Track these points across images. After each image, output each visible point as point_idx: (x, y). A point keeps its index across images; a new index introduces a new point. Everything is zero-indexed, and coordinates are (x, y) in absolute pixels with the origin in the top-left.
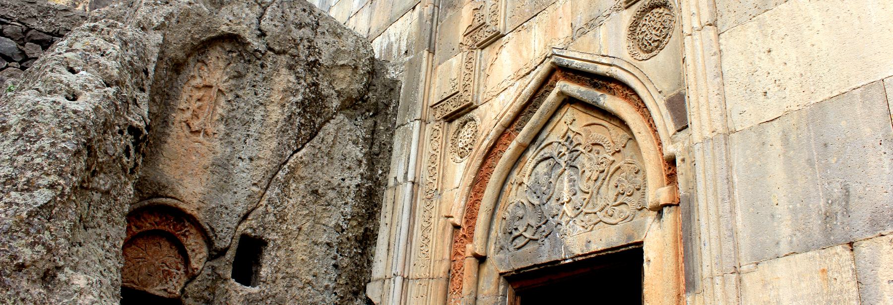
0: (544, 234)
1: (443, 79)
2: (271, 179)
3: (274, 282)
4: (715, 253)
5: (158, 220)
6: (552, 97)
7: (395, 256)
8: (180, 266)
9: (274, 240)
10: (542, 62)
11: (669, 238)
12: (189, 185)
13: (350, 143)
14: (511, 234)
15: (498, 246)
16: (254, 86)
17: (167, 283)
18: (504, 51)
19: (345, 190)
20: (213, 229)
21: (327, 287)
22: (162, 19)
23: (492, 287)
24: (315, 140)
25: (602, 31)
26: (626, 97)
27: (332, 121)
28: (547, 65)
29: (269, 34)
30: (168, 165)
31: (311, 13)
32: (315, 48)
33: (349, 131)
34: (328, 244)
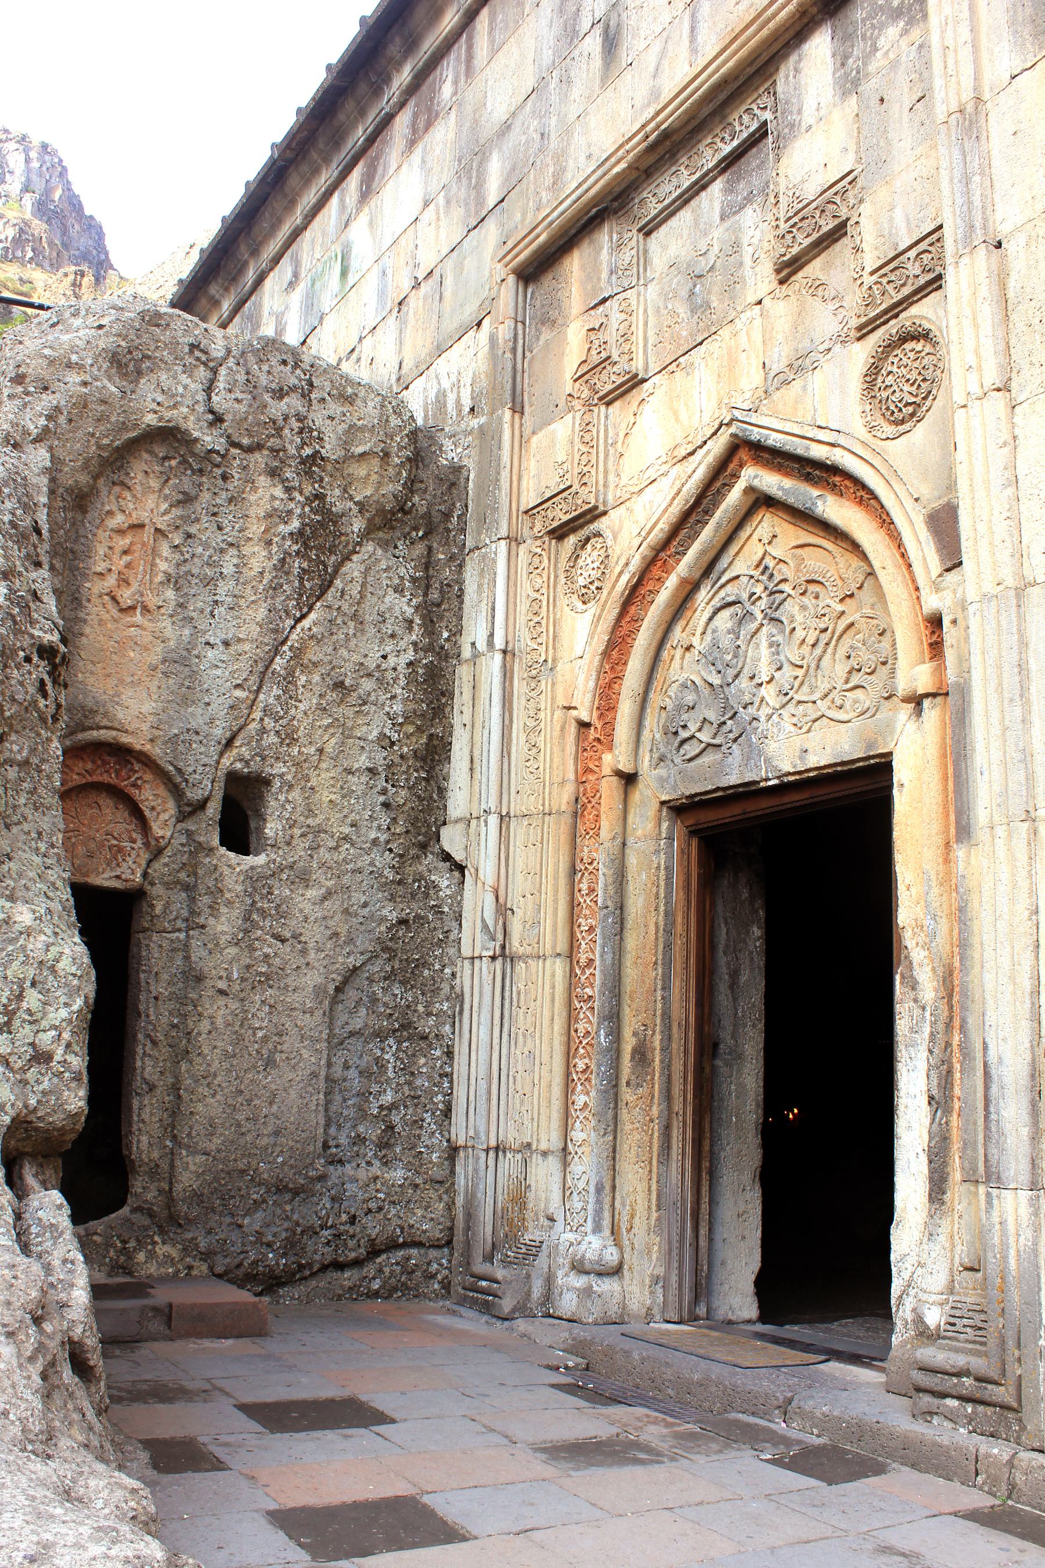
0: (731, 736)
1: (542, 461)
3: (288, 844)
5: (89, 766)
6: (734, 496)
7: (484, 780)
8: (134, 835)
9: (282, 776)
10: (715, 433)
12: (131, 703)
13: (390, 591)
15: (656, 756)
16: (214, 514)
17: (118, 865)
19: (390, 675)
20: (179, 771)
21: (375, 842)
22: (42, 421)
23: (650, 826)
25: (817, 380)
26: (860, 502)
27: (355, 558)
29: (228, 417)
30: (92, 673)
31: (296, 366)
32: (311, 430)
33: (385, 570)
34: (370, 770)
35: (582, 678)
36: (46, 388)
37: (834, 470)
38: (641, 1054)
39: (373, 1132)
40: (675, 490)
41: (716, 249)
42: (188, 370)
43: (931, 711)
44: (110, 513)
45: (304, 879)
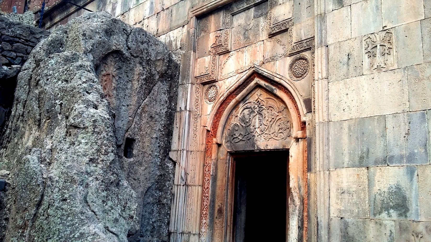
1: (201, 65)
3: (138, 156)
4: (321, 163)
6: (252, 84)
7: (183, 142)
9: (138, 139)
11: (301, 150)
14: (232, 135)
16: (126, 73)
18: (231, 59)
21: (156, 155)
22: (91, 47)
23: (224, 157)
24: (150, 94)
26: (285, 92)
27: (156, 85)
31: (146, 36)
34: (156, 138)
35: (208, 120)
36: (91, 38)
37: (280, 84)
41: (252, 25)
42: (123, 35)
45: (141, 164)
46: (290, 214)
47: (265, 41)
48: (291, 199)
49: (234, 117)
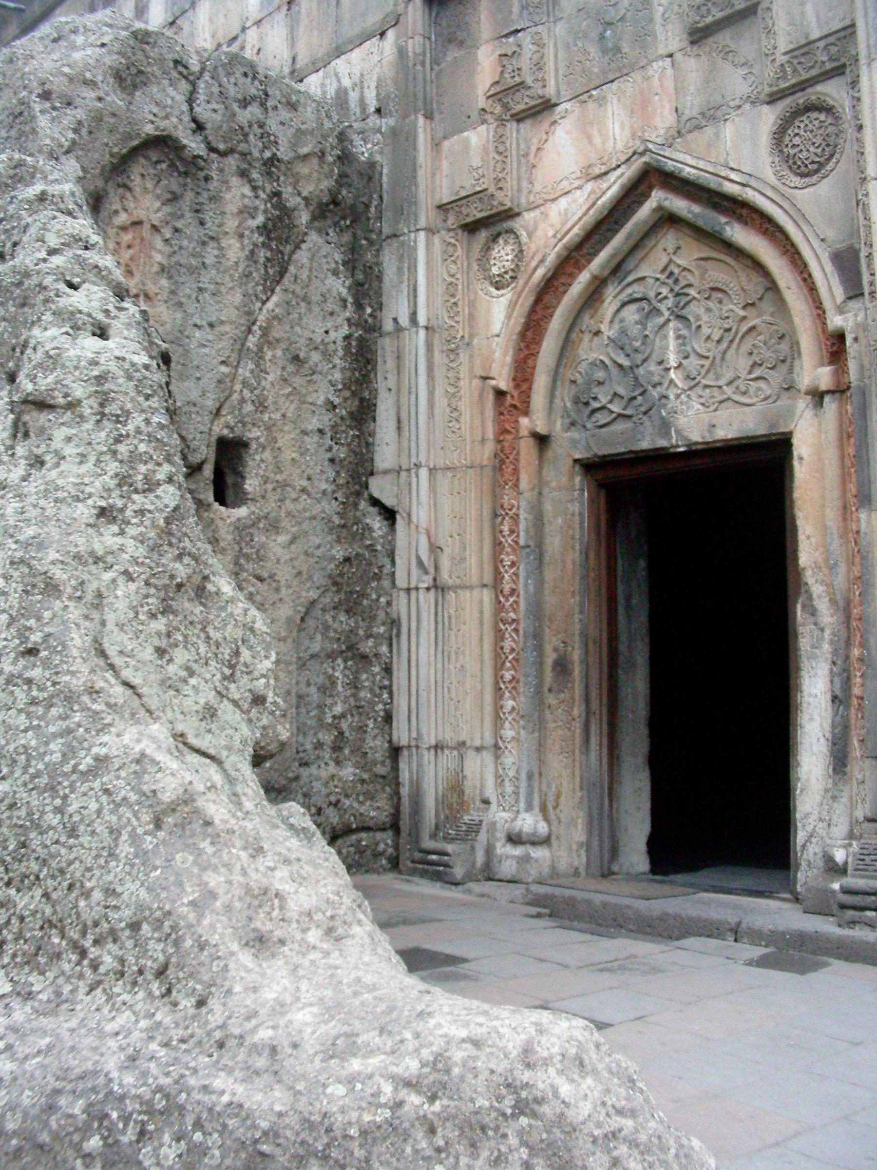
0: (643, 409)
1: (456, 161)
2: (240, 350)
3: (263, 497)
6: (645, 211)
7: (413, 437)
13: (329, 274)
15: (567, 421)
16: (197, 211)
19: (331, 347)
21: (324, 492)
22: (71, 135)
23: (564, 479)
25: (728, 131)
26: (764, 233)
27: (304, 246)
28: (637, 164)
29: (209, 126)
31: (254, 78)
32: (269, 135)
36: (69, 104)
38: (562, 667)
39: (327, 738)
40: (591, 202)
43: (830, 405)
44: (116, 212)
45: (275, 527)
46: (804, 659)
47: (678, 56)
48: (804, 607)
49: (587, 337)
